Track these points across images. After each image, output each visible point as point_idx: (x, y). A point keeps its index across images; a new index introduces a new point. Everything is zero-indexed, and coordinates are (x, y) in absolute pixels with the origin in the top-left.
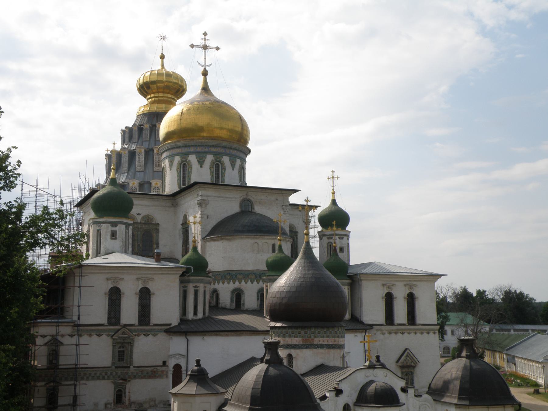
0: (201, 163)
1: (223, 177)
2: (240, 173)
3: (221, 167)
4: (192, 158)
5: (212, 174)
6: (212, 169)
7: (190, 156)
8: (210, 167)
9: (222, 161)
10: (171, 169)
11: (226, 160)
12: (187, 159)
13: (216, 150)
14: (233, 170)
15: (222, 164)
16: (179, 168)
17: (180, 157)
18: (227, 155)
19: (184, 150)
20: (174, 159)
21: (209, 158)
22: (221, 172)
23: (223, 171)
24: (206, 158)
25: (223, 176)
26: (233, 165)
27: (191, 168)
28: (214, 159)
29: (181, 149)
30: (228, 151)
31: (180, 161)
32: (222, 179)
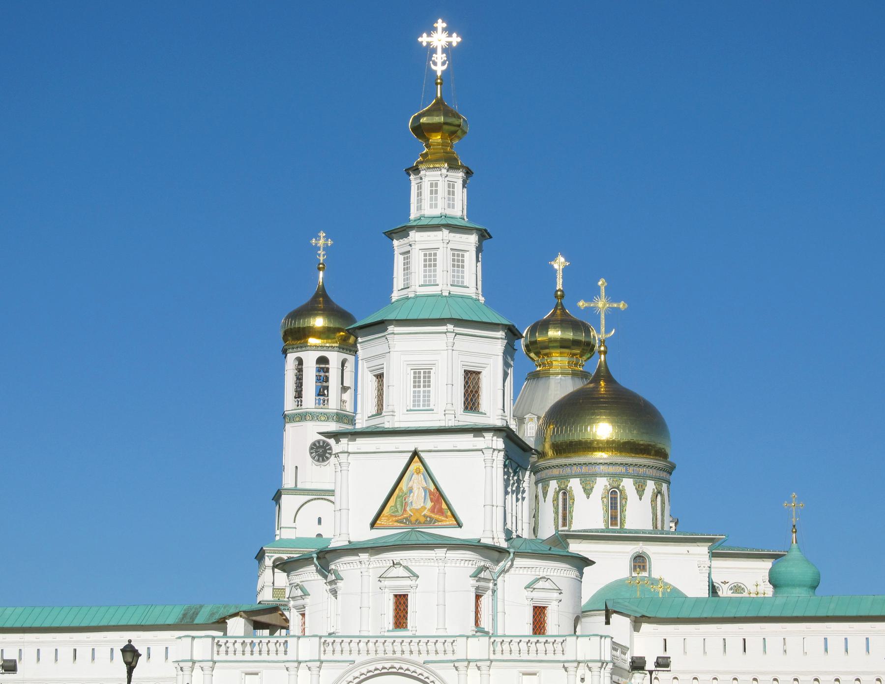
0: (588, 492)
1: (623, 511)
2: (653, 503)
3: (620, 496)
4: (575, 485)
5: (605, 509)
6: (605, 500)
7: (571, 480)
8: (602, 498)
9: (621, 487)
10: (545, 501)
11: (628, 485)
12: (567, 486)
13: (611, 469)
14: (640, 499)
15: (621, 492)
16: (556, 499)
17: (557, 483)
18: (628, 476)
19: (563, 471)
20: (548, 486)
21: (601, 484)
22: (620, 502)
23: (623, 502)
24: (596, 483)
25: (622, 511)
26: (640, 492)
27: (574, 499)
28: (608, 484)
29: (558, 470)
30: (631, 470)
31: (558, 489)
32: (621, 516)
